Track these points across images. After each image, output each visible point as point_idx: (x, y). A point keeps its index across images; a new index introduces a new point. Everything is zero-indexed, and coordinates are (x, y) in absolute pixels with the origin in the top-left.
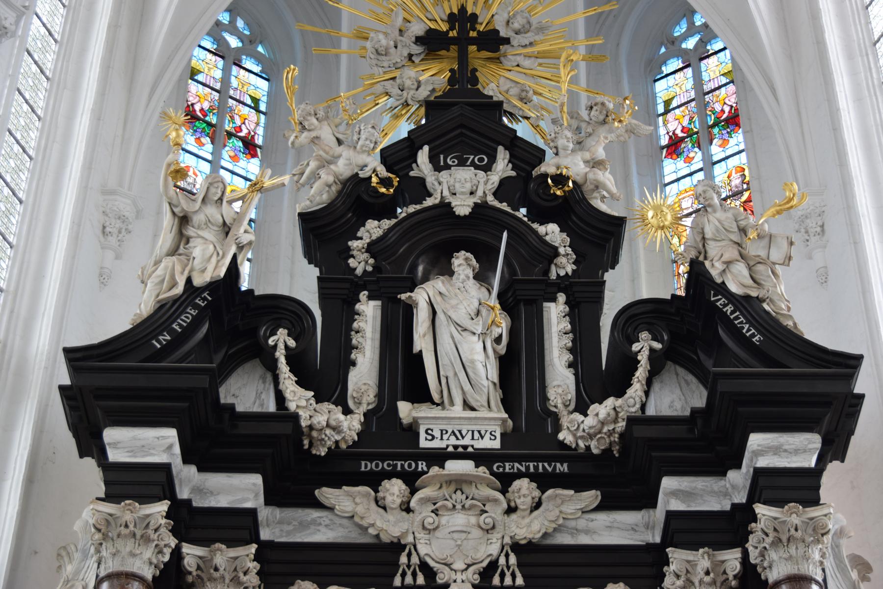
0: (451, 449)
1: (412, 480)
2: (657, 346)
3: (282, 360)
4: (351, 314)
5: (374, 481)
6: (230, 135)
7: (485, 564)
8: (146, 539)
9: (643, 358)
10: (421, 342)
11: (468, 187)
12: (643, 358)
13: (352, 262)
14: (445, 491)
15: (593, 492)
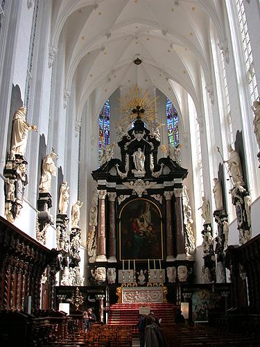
5: (129, 181)
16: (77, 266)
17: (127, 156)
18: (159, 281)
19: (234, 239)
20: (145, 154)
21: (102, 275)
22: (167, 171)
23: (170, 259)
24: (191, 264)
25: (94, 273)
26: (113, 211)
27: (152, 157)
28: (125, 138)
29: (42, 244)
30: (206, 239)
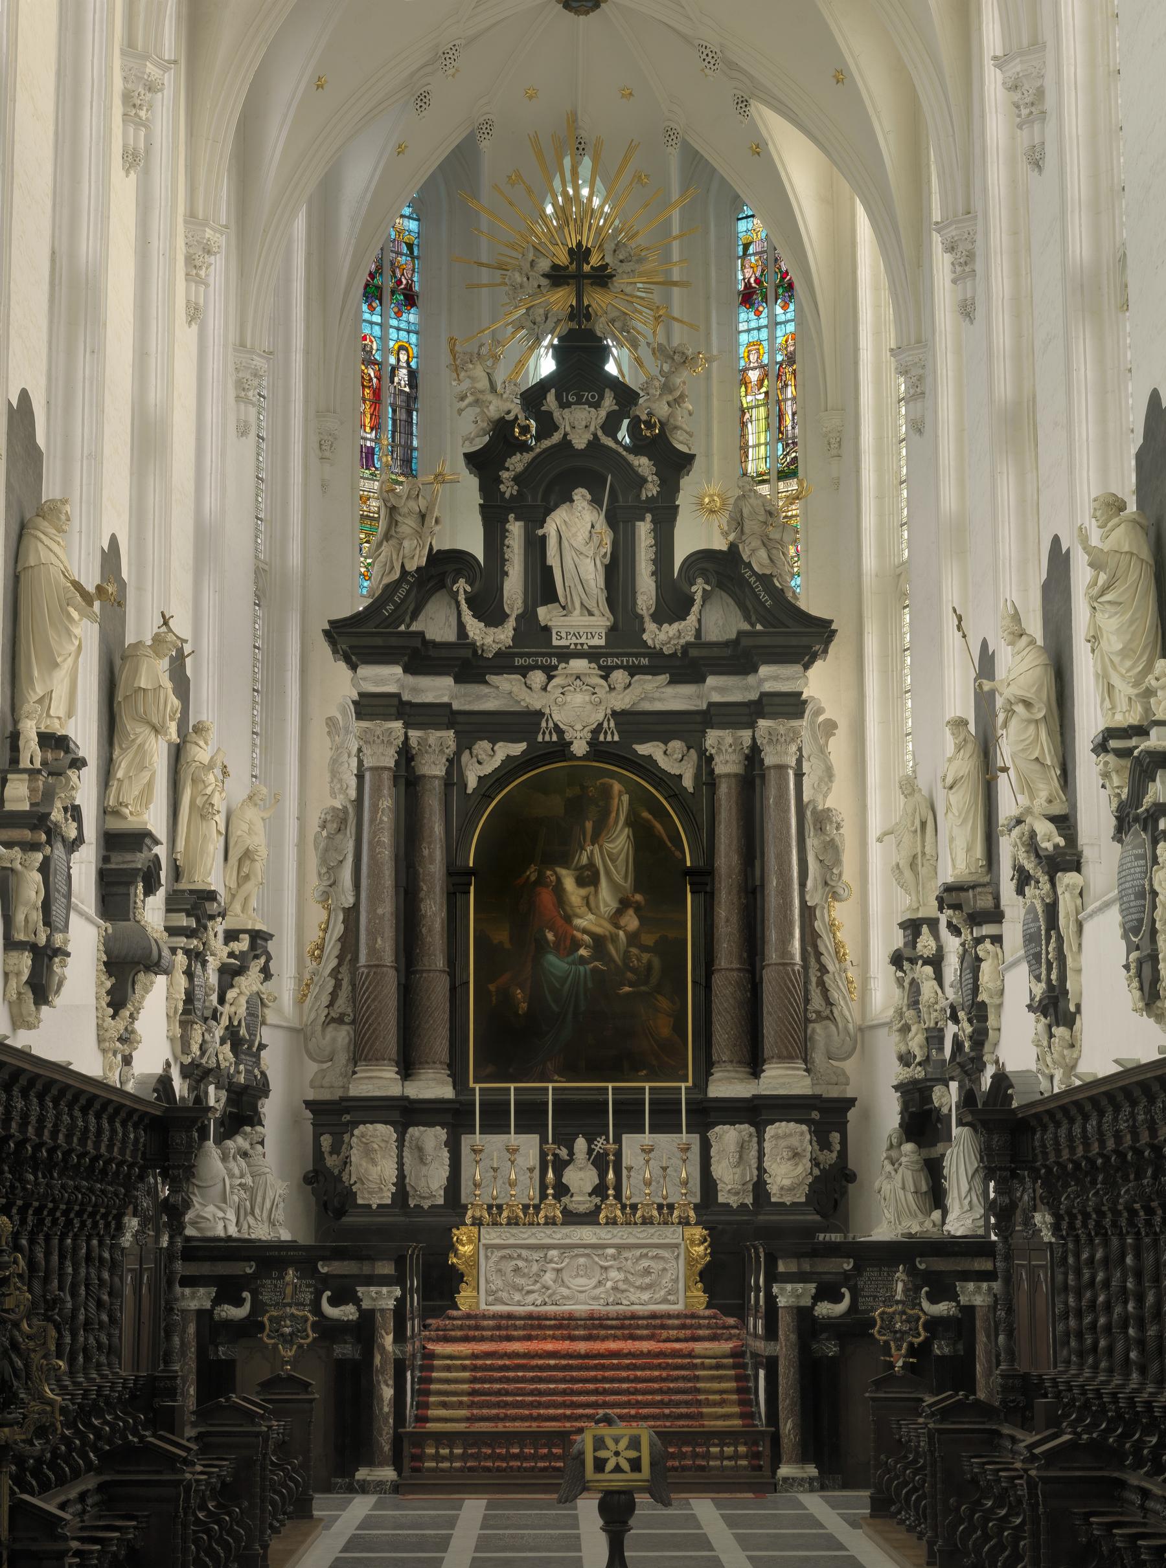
0: (572, 647)
2: (708, 588)
3: (463, 602)
4: (504, 533)
5: (524, 671)
7: (594, 726)
8: (390, 743)
9: (698, 598)
10: (552, 559)
11: (584, 423)
12: (698, 598)
13: (502, 488)
14: (570, 680)
15: (662, 677)
16: (254, 1119)
17: (516, 529)
18: (675, 1196)
20: (612, 521)
25: (336, 1149)
26: (435, 826)
27: (644, 530)
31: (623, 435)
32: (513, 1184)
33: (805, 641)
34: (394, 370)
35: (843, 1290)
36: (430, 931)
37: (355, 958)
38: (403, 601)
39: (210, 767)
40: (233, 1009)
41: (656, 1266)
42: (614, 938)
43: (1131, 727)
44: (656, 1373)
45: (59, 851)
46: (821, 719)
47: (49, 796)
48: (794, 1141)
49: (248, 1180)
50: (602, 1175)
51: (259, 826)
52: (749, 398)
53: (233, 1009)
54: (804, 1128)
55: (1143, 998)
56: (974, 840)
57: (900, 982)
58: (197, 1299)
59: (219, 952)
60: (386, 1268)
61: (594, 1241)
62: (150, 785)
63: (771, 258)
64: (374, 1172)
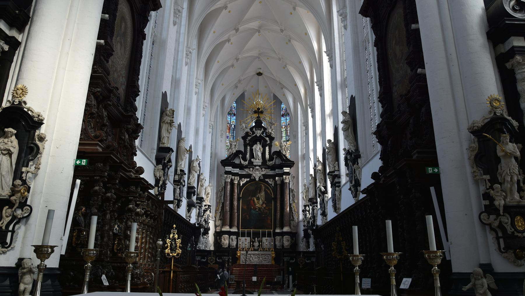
1: (253, 168)
5: (249, 168)
6: (232, 114)
9: (275, 158)
12: (275, 158)
13: (247, 142)
16: (208, 233)
17: (249, 147)
19: (319, 222)
20: (262, 147)
21: (225, 241)
22: (278, 161)
23: (278, 231)
24: (293, 235)
26: (236, 191)
27: (267, 148)
28: (247, 133)
29: (188, 220)
30: (305, 215)
31: (264, 135)
32: (246, 245)
33: (290, 164)
34: (232, 125)
35: (294, 258)
36: (235, 206)
37: (223, 210)
38: (232, 157)
39: (203, 179)
40: (205, 216)
41: (267, 257)
42: (262, 208)
43: (332, 171)
44: (266, 272)
45: (182, 186)
46: (292, 176)
47: (181, 178)
48: (288, 239)
49: (206, 242)
50: (259, 243)
51: (210, 190)
52: (283, 130)
53: (205, 216)
54: (289, 237)
55: (334, 210)
56: (313, 192)
57: (304, 214)
58: (198, 258)
59: (203, 208)
60: (226, 254)
61: (258, 253)
62: (195, 180)
63: (286, 110)
64: (225, 242)
